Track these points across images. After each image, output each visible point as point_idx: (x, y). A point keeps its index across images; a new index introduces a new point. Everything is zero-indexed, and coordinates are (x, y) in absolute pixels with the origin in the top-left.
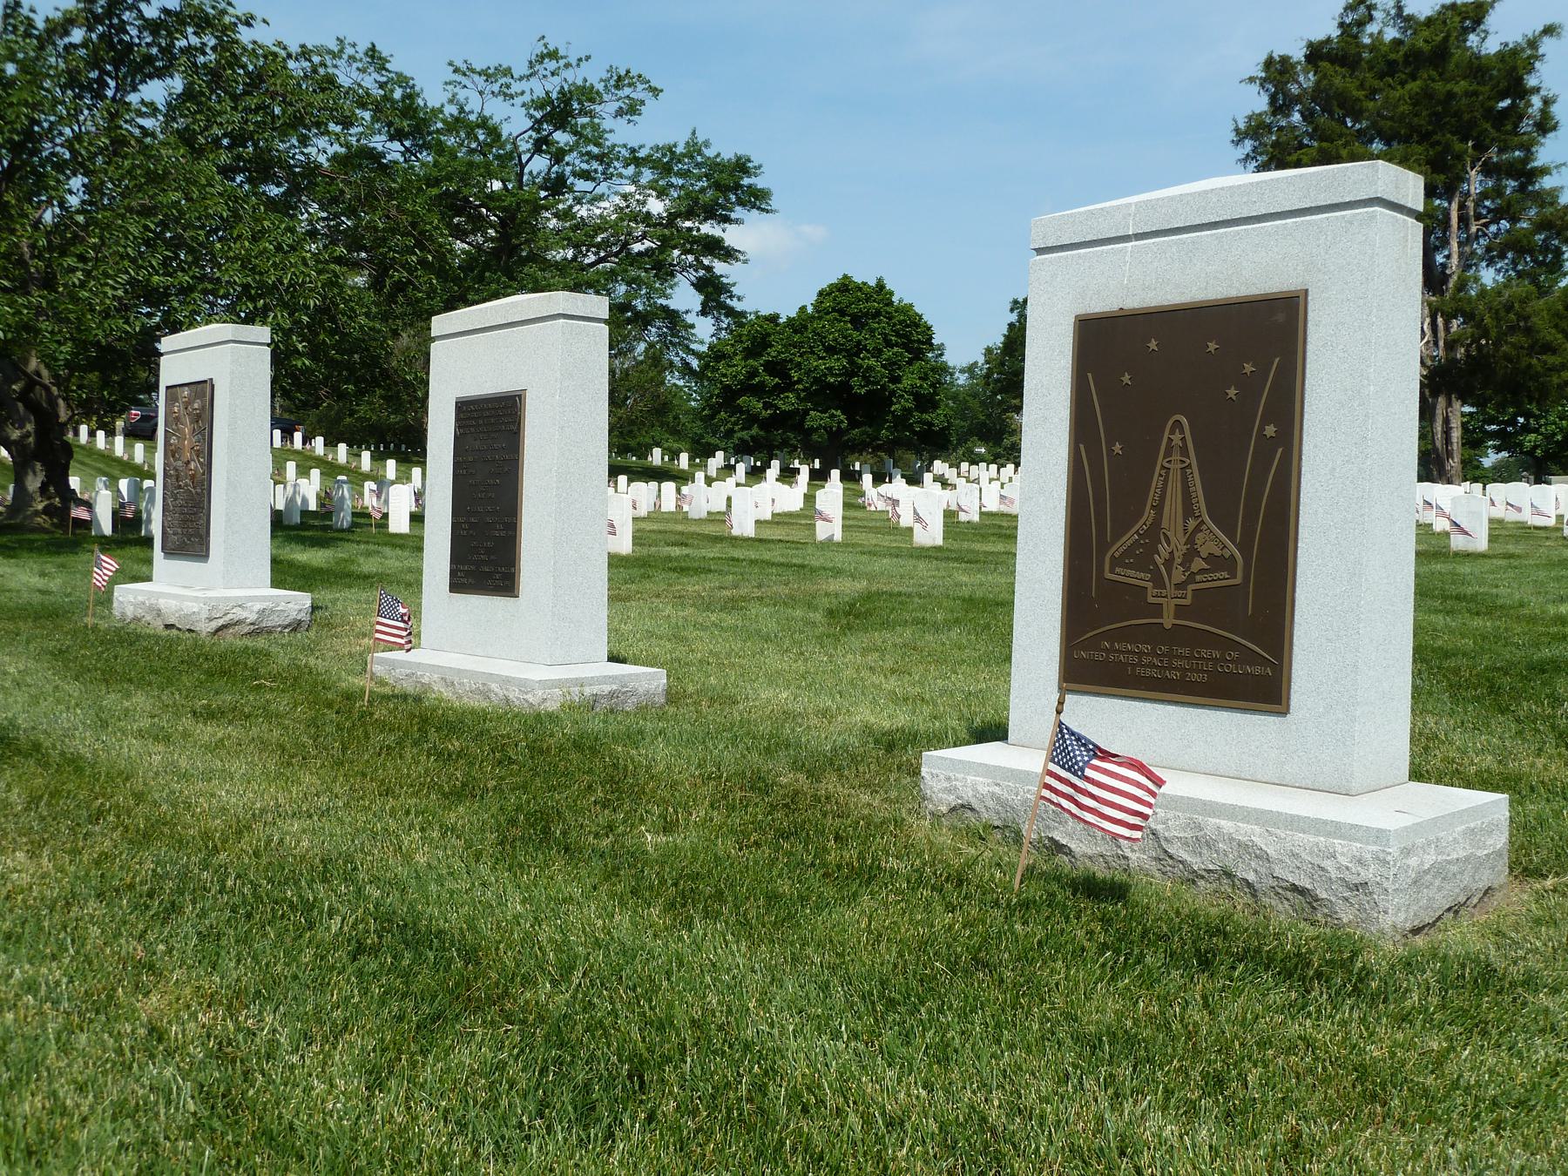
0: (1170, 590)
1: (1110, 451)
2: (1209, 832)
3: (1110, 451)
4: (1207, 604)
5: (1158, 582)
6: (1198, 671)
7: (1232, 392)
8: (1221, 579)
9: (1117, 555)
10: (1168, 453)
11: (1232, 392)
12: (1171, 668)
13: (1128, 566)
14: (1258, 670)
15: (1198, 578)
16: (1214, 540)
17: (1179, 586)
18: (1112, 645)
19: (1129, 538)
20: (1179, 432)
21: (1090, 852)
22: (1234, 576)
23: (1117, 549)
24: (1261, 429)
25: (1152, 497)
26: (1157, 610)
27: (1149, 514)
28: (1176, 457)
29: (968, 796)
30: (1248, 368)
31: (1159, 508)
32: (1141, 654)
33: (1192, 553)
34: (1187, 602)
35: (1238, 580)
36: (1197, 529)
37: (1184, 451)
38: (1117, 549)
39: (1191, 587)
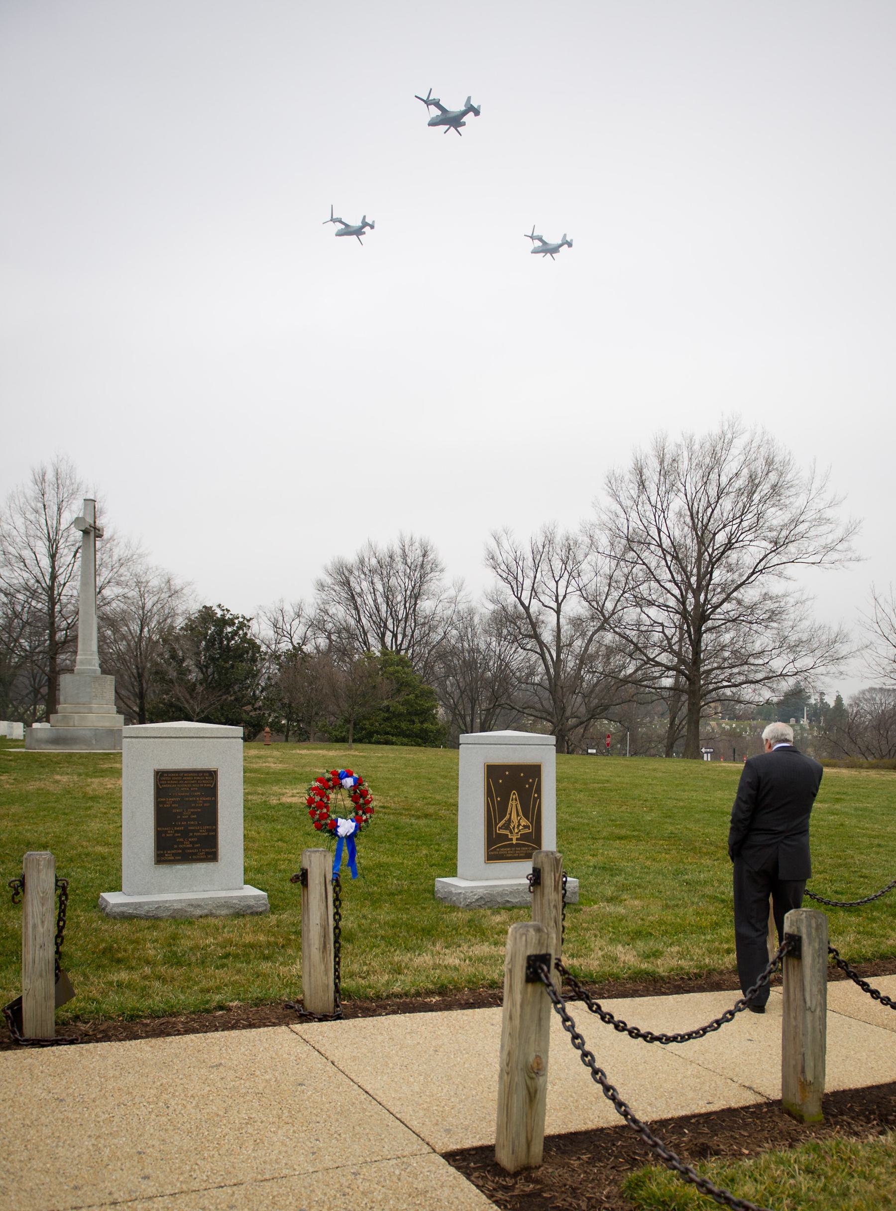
4: (524, 837)
5: (511, 833)
8: (527, 831)
16: (524, 822)
19: (503, 822)
20: (514, 795)
23: (500, 825)
26: (511, 840)
27: (508, 816)
31: (510, 814)
33: (519, 825)
38: (500, 825)
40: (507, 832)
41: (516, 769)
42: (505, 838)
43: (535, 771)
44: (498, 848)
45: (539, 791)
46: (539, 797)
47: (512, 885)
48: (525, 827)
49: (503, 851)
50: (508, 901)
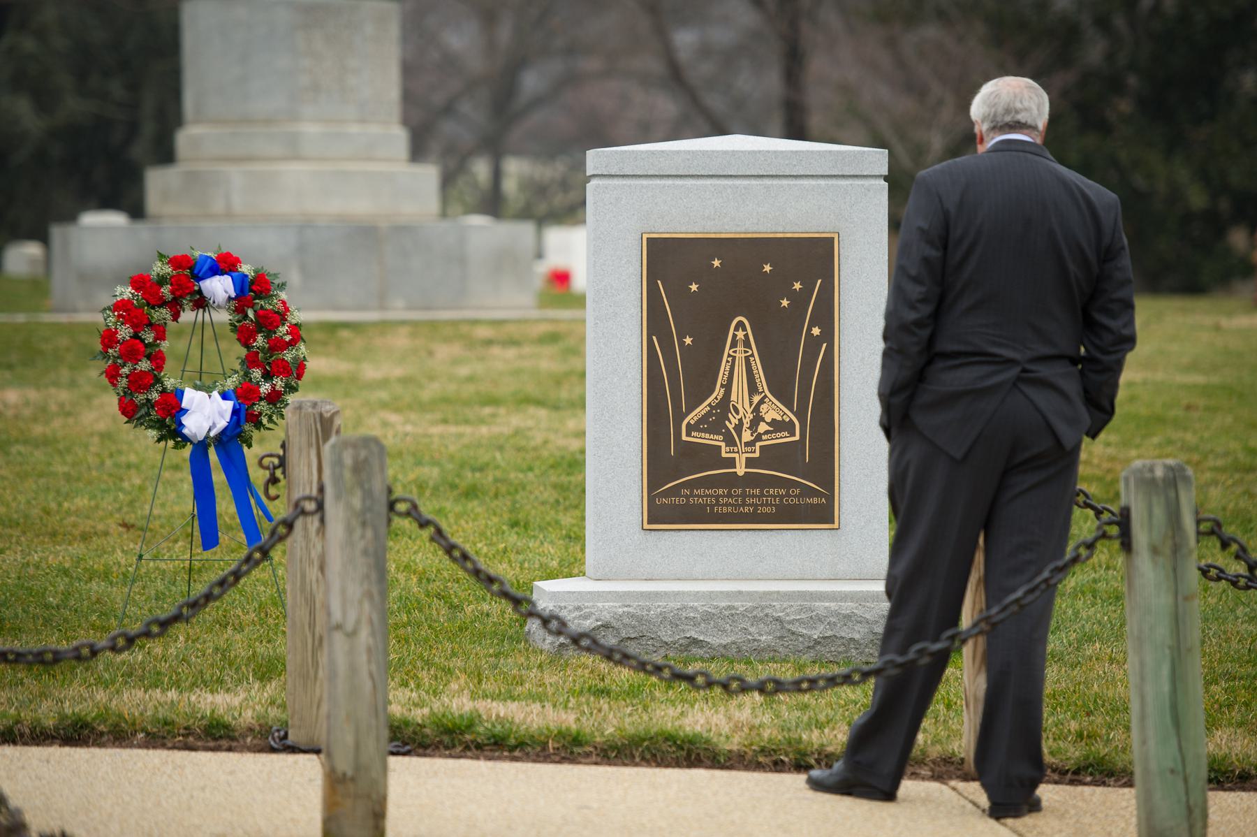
1: (681, 343)
2: (822, 612)
3: (681, 343)
4: (771, 456)
5: (730, 441)
6: (767, 505)
7: (785, 303)
8: (783, 438)
10: (734, 344)
11: (785, 303)
12: (744, 504)
14: (815, 500)
15: (764, 437)
16: (773, 411)
17: (747, 444)
18: (692, 492)
19: (702, 409)
20: (740, 329)
21: (724, 643)
22: (793, 434)
23: (692, 418)
24: (809, 329)
26: (731, 463)
27: (719, 392)
28: (740, 348)
29: (606, 617)
30: (797, 286)
31: (728, 387)
32: (717, 497)
33: (757, 419)
34: (757, 455)
35: (797, 438)
36: (762, 402)
37: (747, 344)
38: (692, 418)
39: (758, 444)
40: (716, 440)
41: (745, 252)
42: (711, 456)
43: (814, 258)
44: (685, 487)
45: (825, 315)
46: (828, 335)
47: (711, 595)
48: (777, 426)
49: (702, 496)
50: (695, 642)
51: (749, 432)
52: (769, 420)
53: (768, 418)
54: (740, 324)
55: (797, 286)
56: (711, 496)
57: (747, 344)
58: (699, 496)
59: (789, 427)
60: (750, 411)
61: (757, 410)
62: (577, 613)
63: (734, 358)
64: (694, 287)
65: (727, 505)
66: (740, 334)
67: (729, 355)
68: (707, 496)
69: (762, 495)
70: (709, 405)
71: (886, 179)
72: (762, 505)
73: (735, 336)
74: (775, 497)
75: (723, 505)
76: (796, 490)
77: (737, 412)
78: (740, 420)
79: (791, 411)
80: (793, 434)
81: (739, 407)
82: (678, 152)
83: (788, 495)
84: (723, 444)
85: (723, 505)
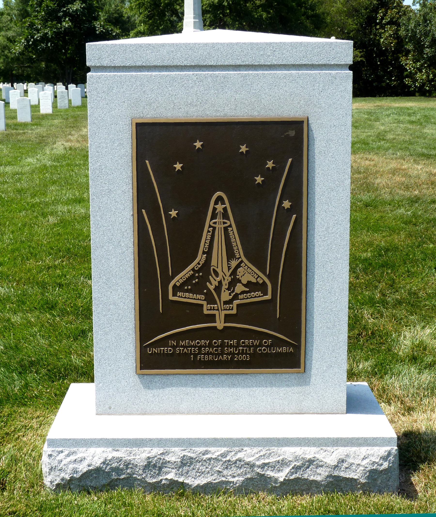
0: (219, 305)
1: (168, 216)
3: (168, 216)
5: (210, 299)
8: (257, 297)
9: (178, 284)
10: (214, 216)
12: (222, 354)
13: (187, 291)
14: (284, 349)
15: (240, 297)
16: (248, 273)
17: (226, 303)
18: (178, 343)
19: (186, 273)
20: (219, 203)
23: (178, 280)
25: (203, 246)
26: (212, 318)
27: (201, 258)
31: (209, 253)
32: (200, 348)
34: (234, 312)
35: (268, 297)
36: (238, 266)
37: (225, 215)
38: (178, 280)
39: (236, 302)
42: (194, 313)
51: (228, 292)
52: (245, 282)
53: (245, 282)
54: (220, 199)
55: (270, 164)
56: (195, 347)
57: (225, 215)
58: (184, 347)
59: (262, 287)
60: (228, 274)
61: (234, 273)
62: (72, 458)
63: (214, 228)
64: (178, 166)
65: (208, 354)
66: (220, 207)
67: (210, 226)
68: (191, 346)
69: (238, 345)
70: (193, 269)
71: (351, 68)
72: (238, 354)
73: (215, 209)
74: (249, 347)
75: (204, 354)
76: (269, 342)
77: (217, 274)
78: (220, 283)
79: (265, 273)
80: (266, 294)
81: (219, 270)
82: (163, 45)
83: (261, 345)
84: (205, 303)
85: (204, 354)
